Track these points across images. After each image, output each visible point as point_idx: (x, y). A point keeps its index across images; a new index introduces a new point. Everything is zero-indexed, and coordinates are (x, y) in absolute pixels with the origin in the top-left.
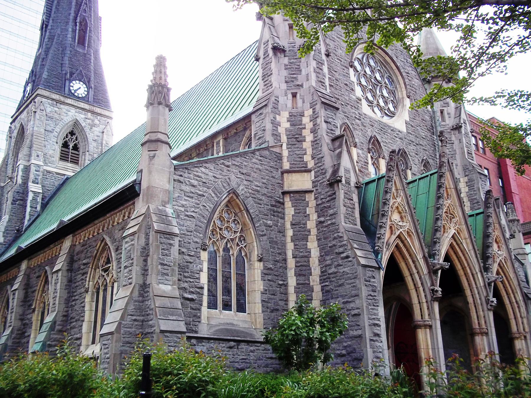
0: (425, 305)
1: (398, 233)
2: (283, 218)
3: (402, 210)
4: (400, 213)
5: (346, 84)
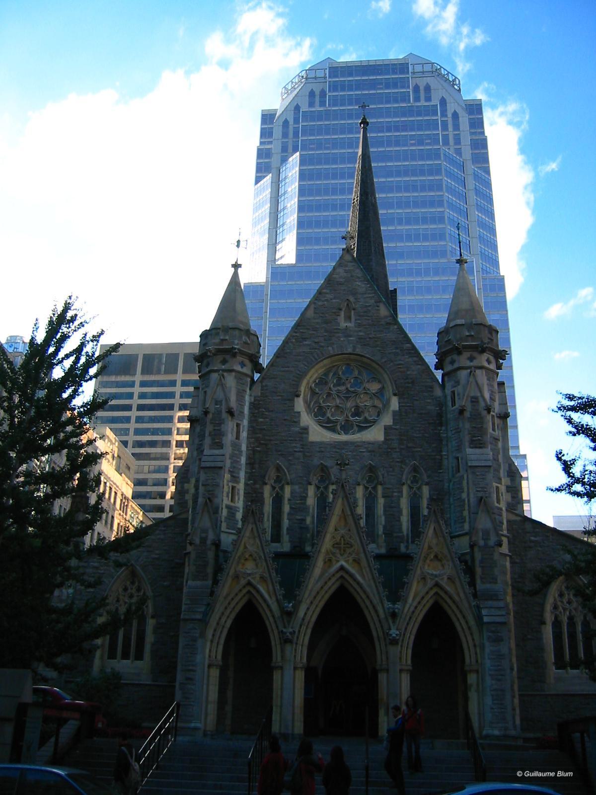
0: (278, 646)
1: (243, 582)
2: (183, 577)
3: (256, 557)
4: (255, 560)
5: (285, 420)
